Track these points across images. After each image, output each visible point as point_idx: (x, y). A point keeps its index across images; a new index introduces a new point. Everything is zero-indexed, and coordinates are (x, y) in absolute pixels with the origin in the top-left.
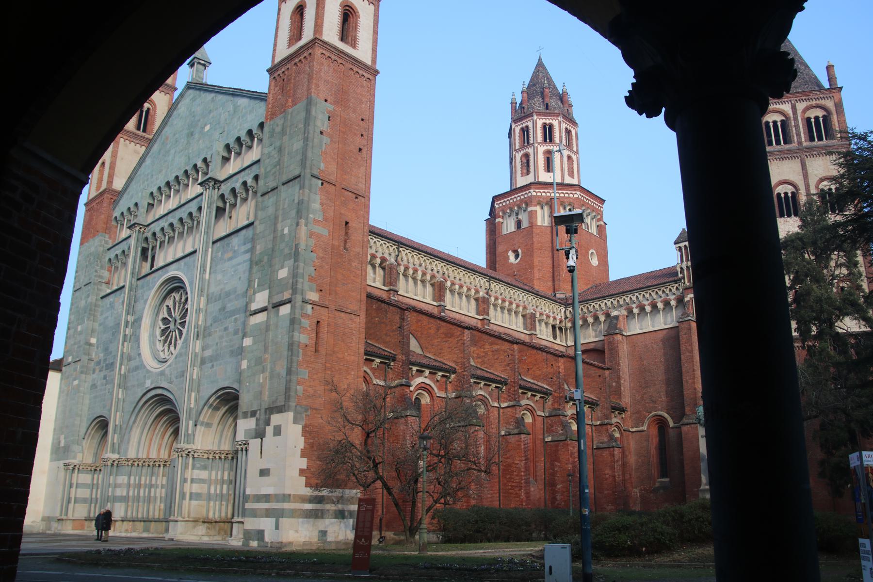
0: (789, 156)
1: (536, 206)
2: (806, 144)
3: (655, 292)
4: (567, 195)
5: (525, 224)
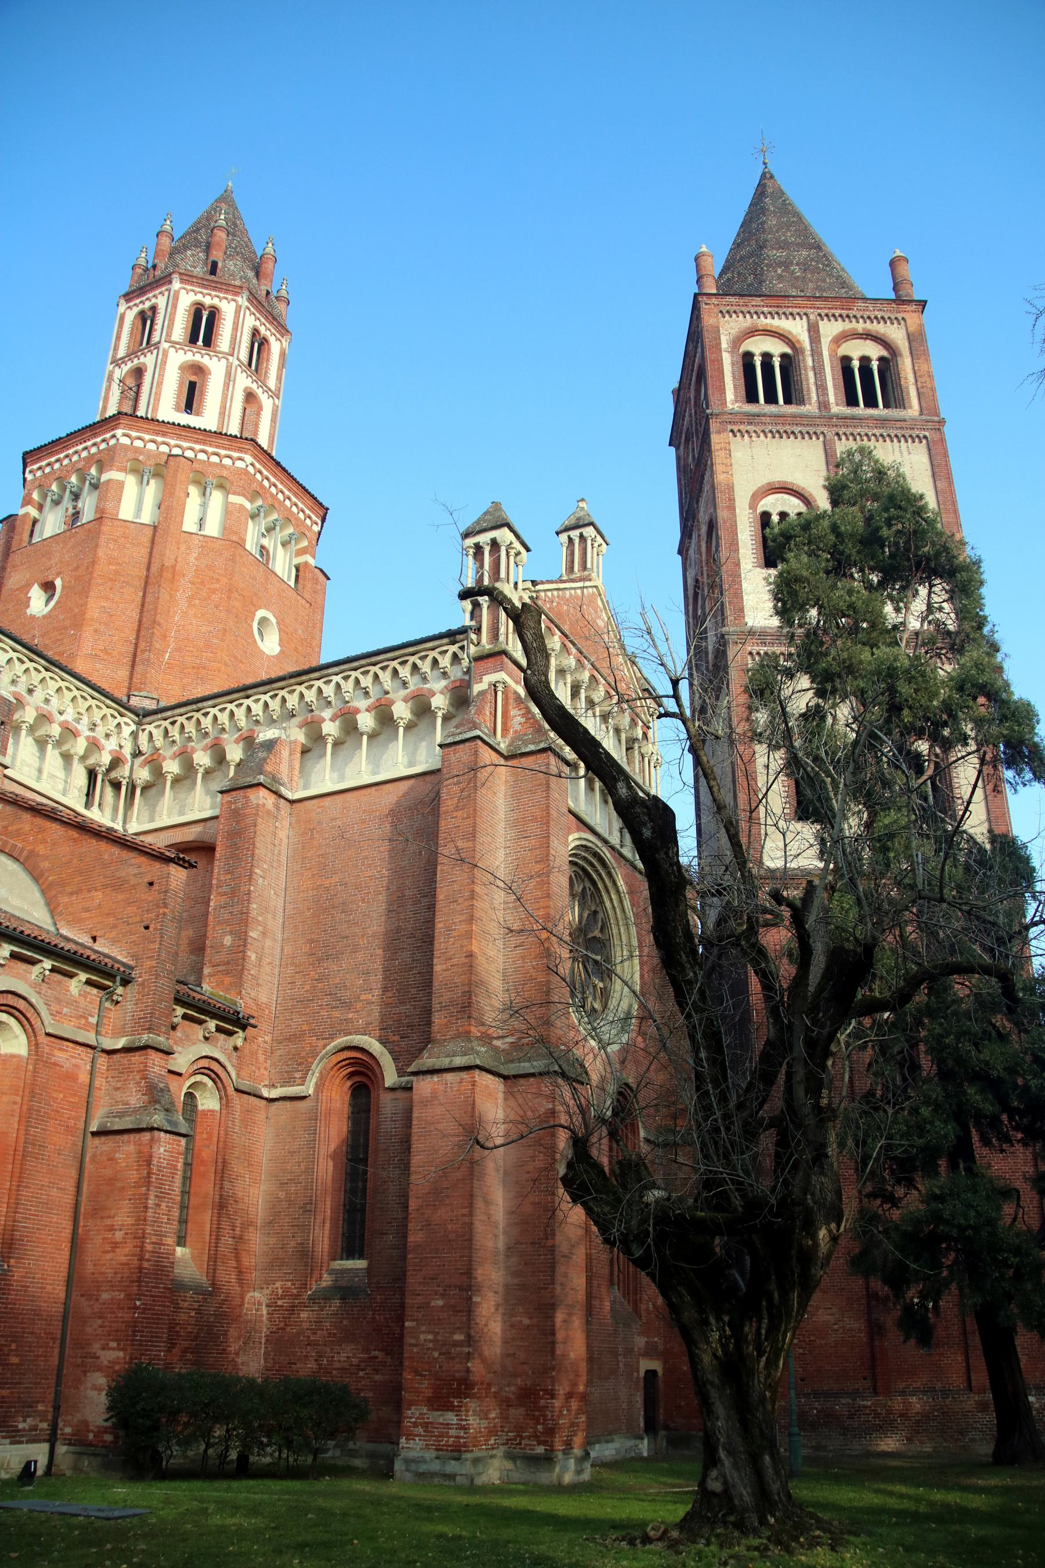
0: (797, 430)
1: (123, 469)
2: (837, 407)
3: (389, 670)
4: (215, 459)
5: (87, 516)
